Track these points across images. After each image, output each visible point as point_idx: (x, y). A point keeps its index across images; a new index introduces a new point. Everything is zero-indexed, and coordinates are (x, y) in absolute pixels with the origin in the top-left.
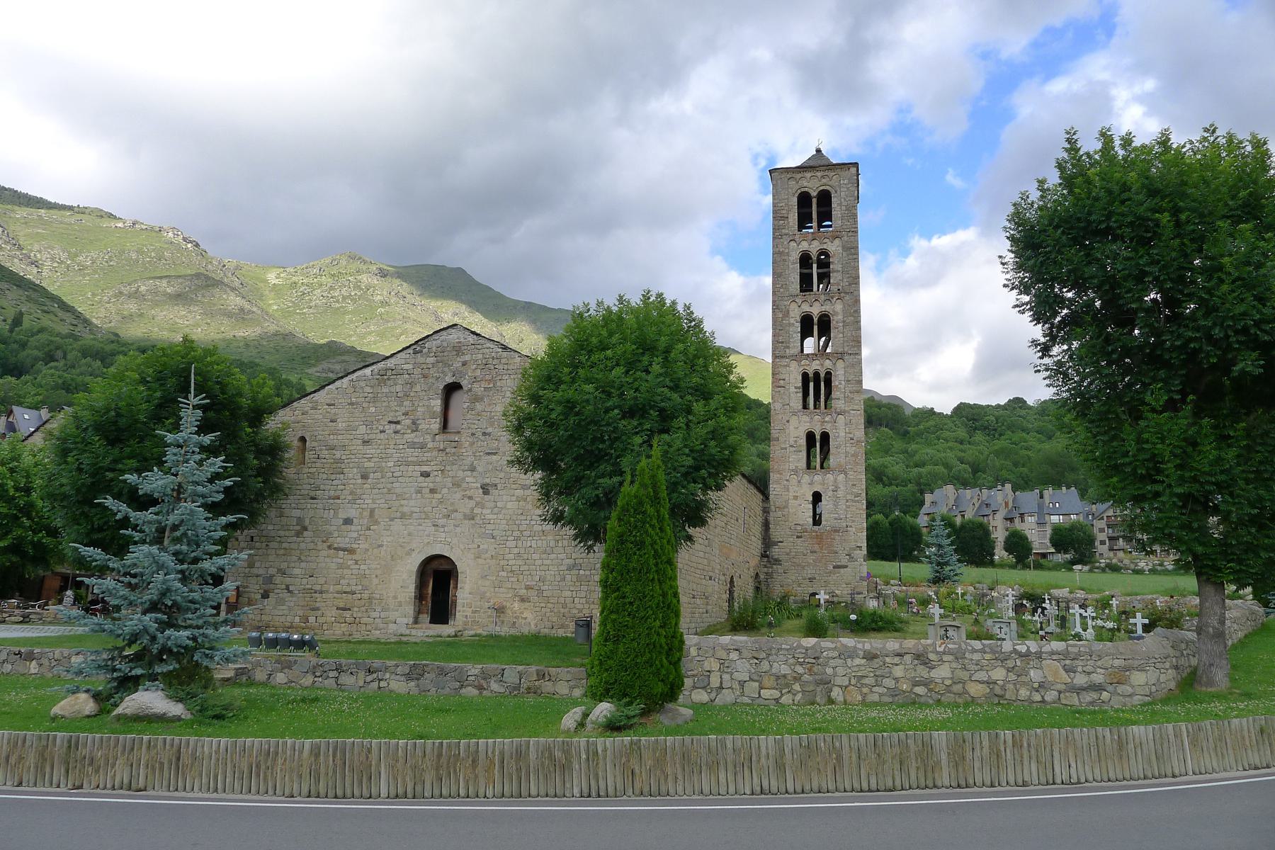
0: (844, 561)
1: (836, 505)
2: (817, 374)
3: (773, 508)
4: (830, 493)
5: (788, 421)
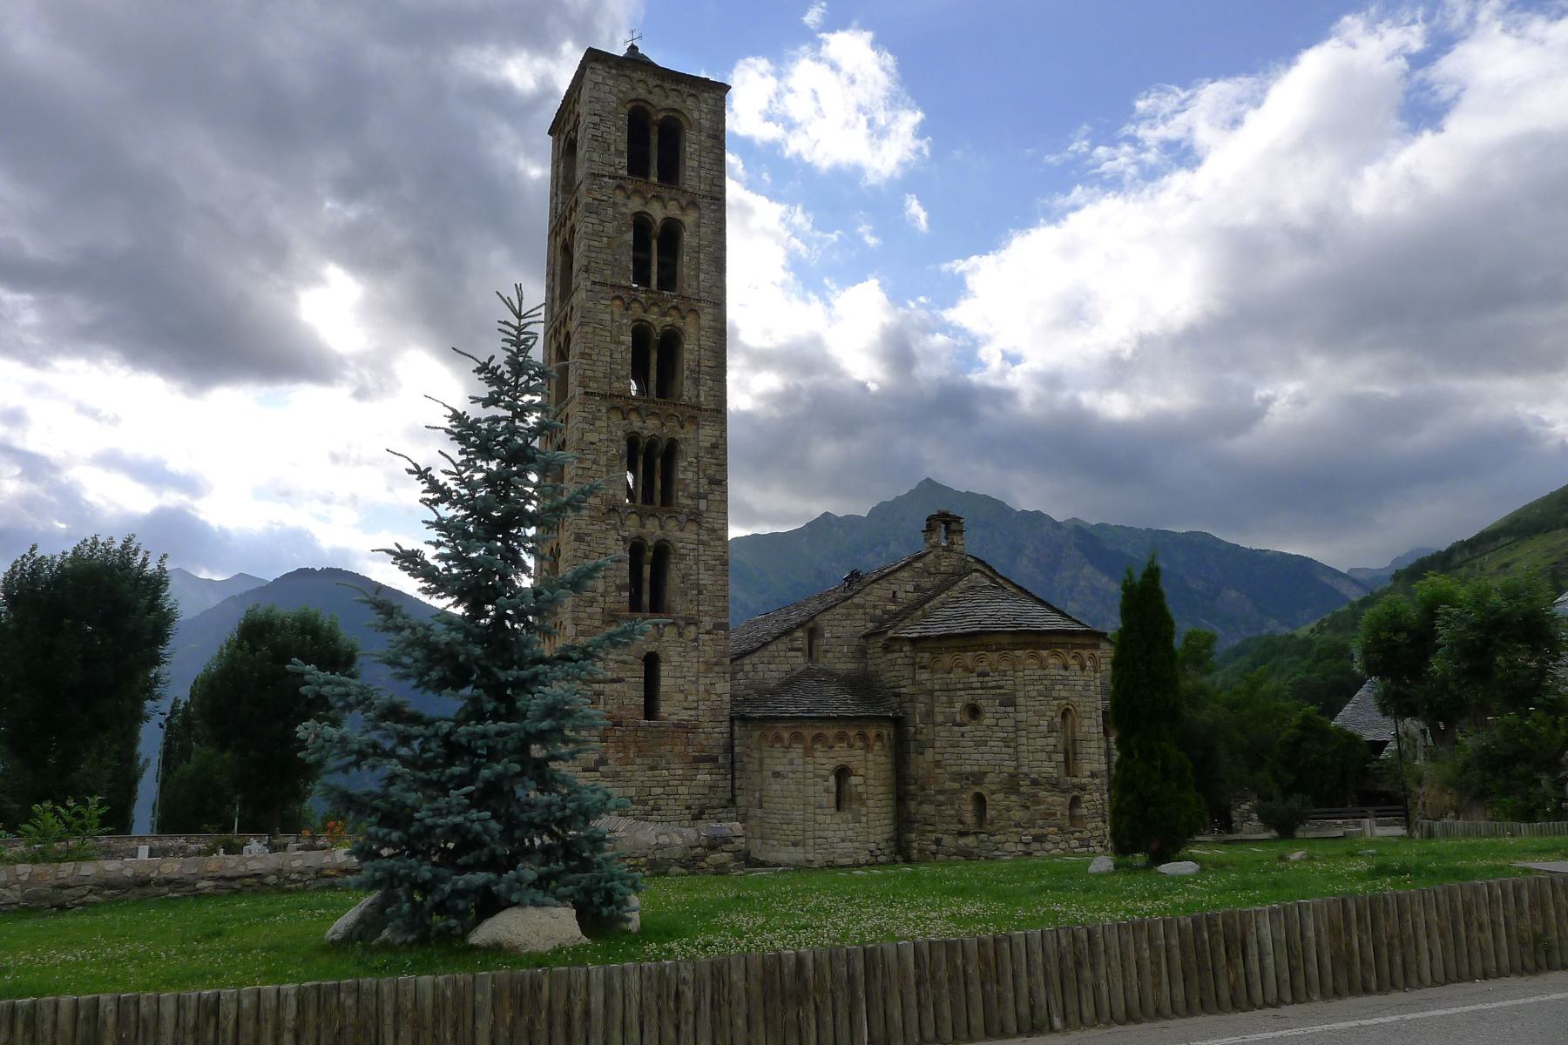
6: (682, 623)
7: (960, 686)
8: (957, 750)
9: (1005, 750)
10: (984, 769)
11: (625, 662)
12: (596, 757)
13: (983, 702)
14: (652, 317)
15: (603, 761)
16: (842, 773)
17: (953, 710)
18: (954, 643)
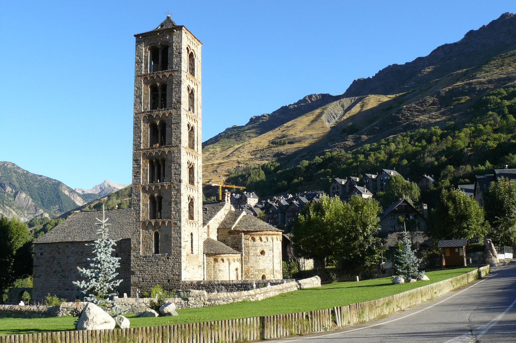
6: (196, 223)
7: (259, 245)
8: (258, 263)
9: (270, 263)
10: (265, 268)
11: (188, 235)
12: (185, 266)
13: (265, 250)
14: (190, 122)
15: (186, 267)
16: (237, 269)
17: (257, 252)
18: (259, 233)
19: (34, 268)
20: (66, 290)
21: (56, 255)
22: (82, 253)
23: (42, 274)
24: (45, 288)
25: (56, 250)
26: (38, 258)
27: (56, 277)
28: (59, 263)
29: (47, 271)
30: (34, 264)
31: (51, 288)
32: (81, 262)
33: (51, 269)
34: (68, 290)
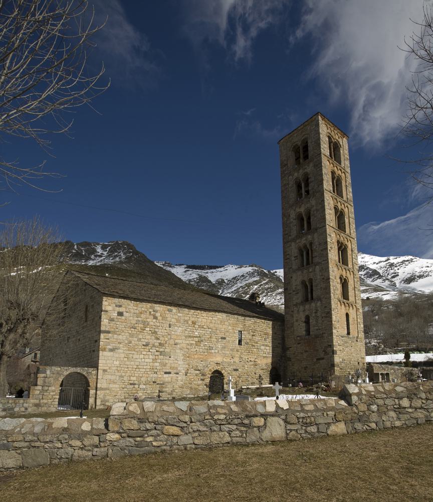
0: (322, 355)
1: (317, 321)
2: (305, 246)
3: (286, 328)
4: (314, 315)
5: (292, 277)
19: (102, 336)
20: (166, 373)
21: (148, 320)
22: (194, 323)
23: (121, 346)
24: (126, 369)
25: (150, 312)
26: (111, 320)
27: (150, 353)
28: (155, 333)
29: (130, 342)
30: (103, 328)
31: (137, 370)
32: (192, 335)
33: (139, 340)
34: (170, 373)
